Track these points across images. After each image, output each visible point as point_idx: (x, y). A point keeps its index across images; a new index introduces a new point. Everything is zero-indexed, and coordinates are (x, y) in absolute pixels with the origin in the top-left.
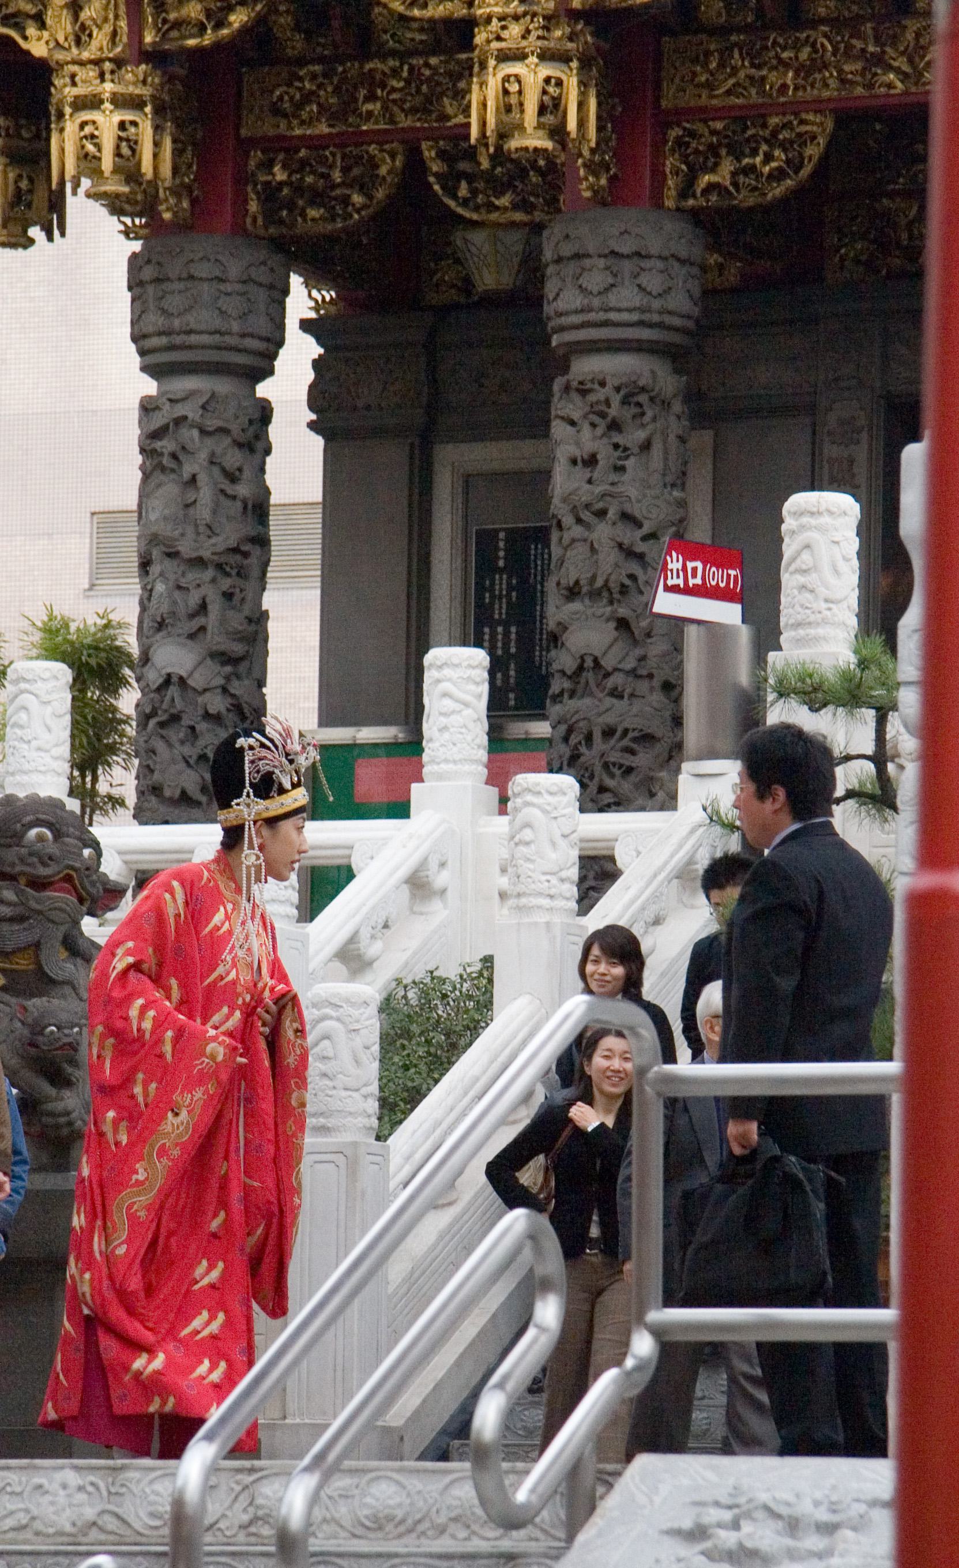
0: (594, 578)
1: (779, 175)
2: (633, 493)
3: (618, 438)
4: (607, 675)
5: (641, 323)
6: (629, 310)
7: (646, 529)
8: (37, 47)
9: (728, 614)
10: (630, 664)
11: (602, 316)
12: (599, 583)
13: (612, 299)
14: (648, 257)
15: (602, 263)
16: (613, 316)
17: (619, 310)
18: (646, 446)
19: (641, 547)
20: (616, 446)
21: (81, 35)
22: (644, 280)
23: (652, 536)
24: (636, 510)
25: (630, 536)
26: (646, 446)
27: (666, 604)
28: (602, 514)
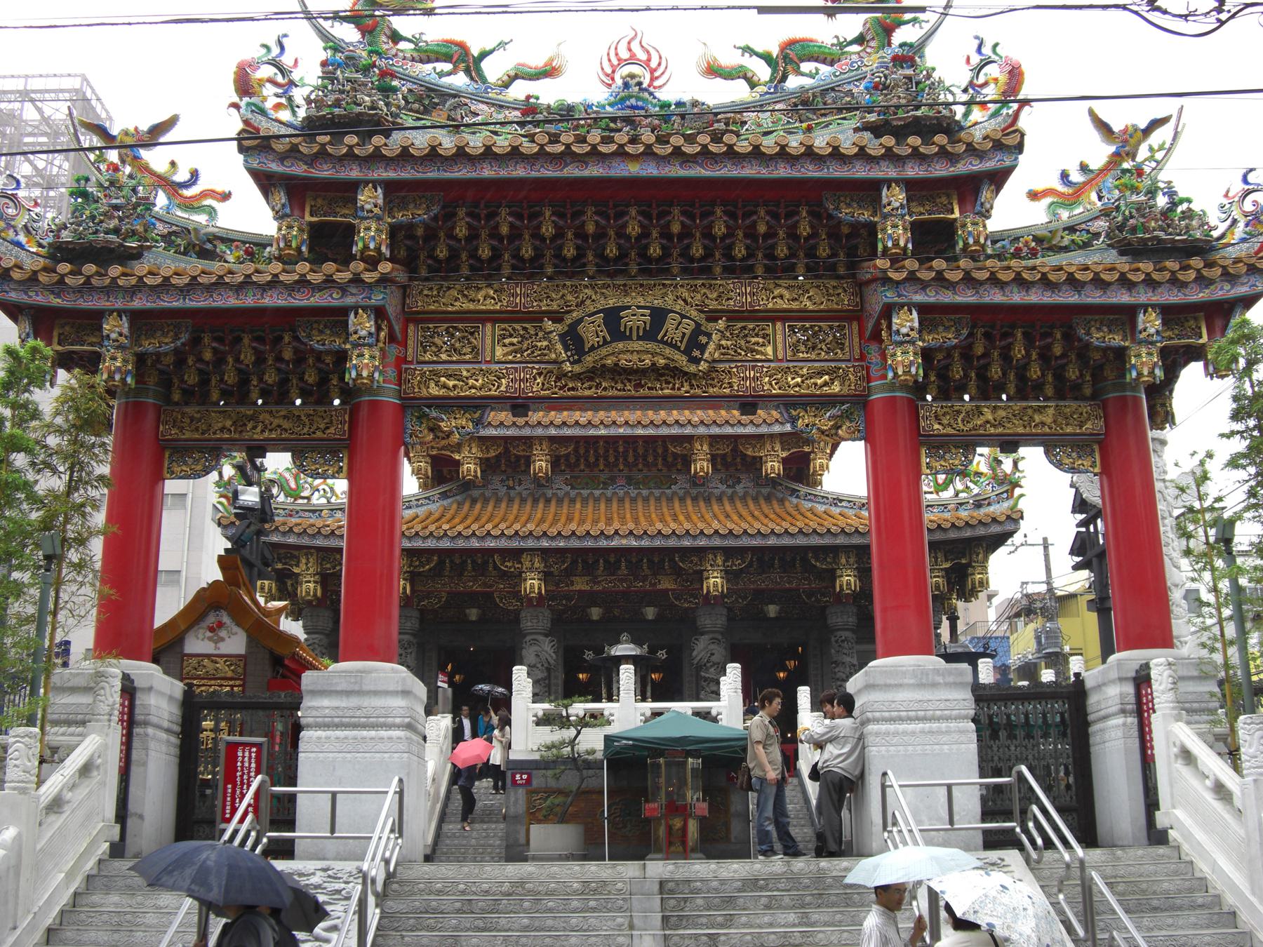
8: (296, 570)
9: (446, 686)
21: (308, 569)
27: (440, 684)
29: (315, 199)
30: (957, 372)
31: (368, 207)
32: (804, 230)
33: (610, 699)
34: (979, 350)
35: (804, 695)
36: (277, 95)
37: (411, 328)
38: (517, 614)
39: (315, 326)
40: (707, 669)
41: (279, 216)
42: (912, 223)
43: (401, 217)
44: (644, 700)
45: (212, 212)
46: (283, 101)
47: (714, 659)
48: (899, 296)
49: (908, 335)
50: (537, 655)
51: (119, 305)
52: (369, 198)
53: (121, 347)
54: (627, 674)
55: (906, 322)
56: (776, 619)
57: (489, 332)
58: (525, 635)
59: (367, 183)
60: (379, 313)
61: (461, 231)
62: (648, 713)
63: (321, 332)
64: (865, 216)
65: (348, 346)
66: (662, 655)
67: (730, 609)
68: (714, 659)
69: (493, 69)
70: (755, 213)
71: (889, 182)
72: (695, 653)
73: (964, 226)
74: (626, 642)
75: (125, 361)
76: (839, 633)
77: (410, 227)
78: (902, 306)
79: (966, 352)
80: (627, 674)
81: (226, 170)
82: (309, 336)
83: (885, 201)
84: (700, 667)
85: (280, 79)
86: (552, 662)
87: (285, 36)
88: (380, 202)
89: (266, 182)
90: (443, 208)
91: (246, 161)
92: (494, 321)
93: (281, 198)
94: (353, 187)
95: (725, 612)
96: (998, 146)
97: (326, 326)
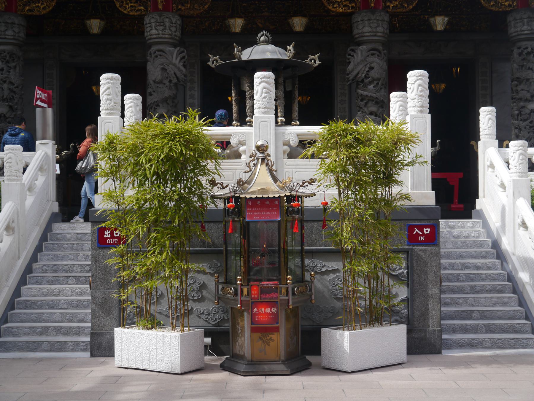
0: (3, 96)
1: (44, 8)
2: (12, 77)
3: (9, 65)
4: (7, 118)
5: (14, 39)
6: (11, 36)
7: (16, 85)
10: (12, 116)
11: (4, 36)
12: (5, 97)
13: (7, 33)
14: (15, 24)
15: (4, 24)
16: (7, 37)
17: (8, 35)
18: (15, 67)
19: (15, 90)
20: (8, 66)
22: (14, 29)
23: (17, 87)
24: (13, 81)
25: (12, 87)
26: (15, 67)
28: (5, 82)
33: (243, 121)
35: (487, 117)
38: (140, 19)
40: (365, 86)
44: (288, 122)
47: (374, 74)
50: (164, 69)
54: (263, 84)
56: (446, 30)
58: (150, 47)
62: (294, 142)
66: (314, 60)
67: (393, 16)
68: (373, 74)
72: (350, 67)
74: (266, 42)
76: (524, 44)
80: (263, 84)
84: (359, 82)
86: (181, 76)
95: (387, 18)
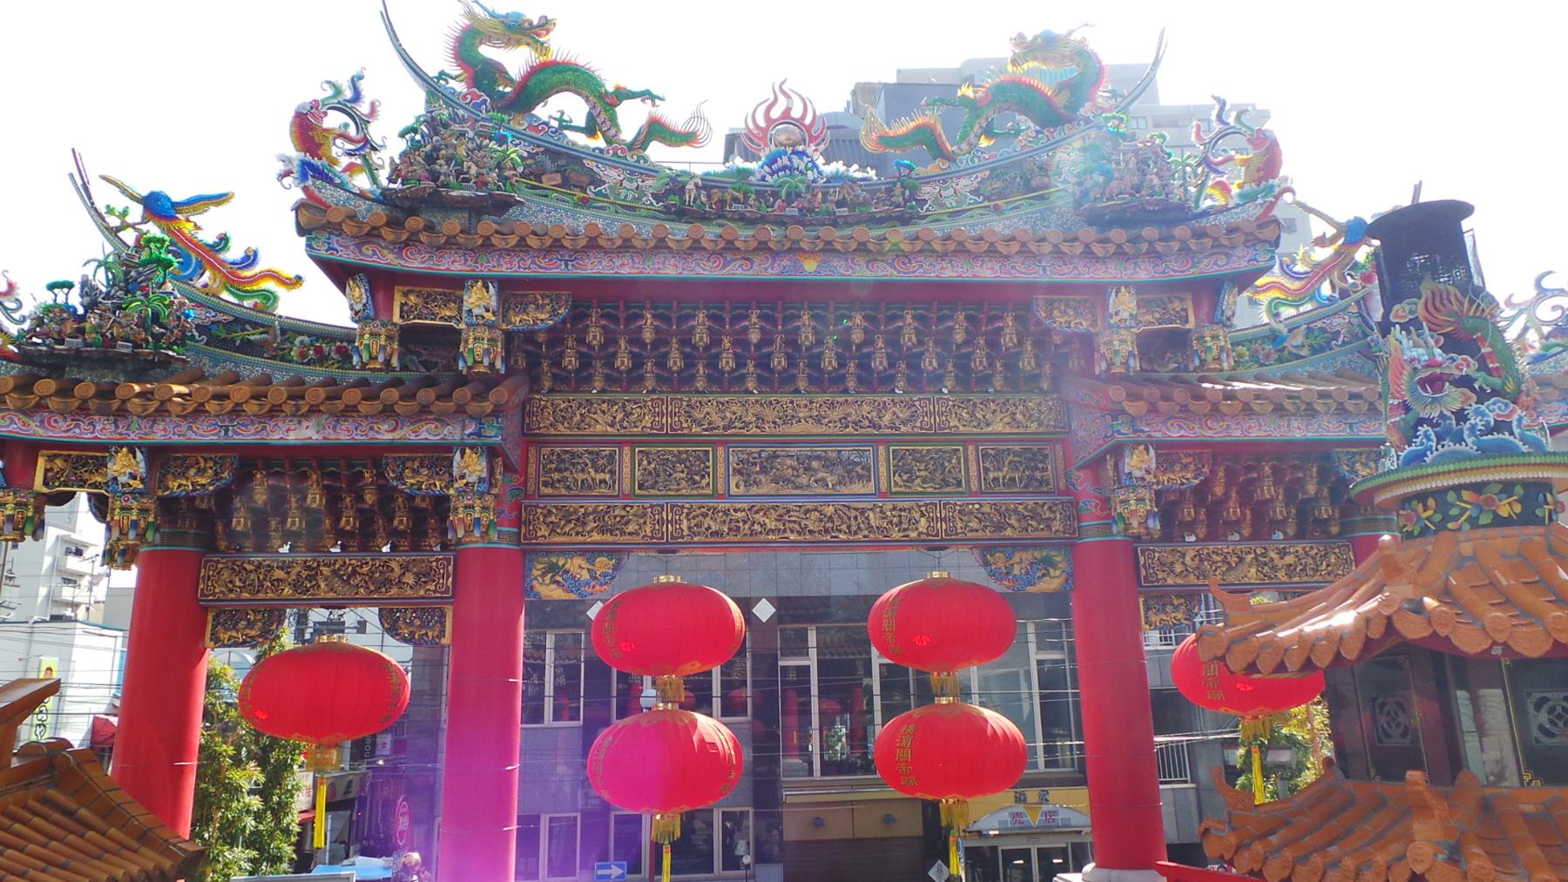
29: (406, 294)
30: (1188, 513)
31: (476, 311)
32: (1008, 339)
34: (1219, 490)
36: (350, 154)
37: (532, 450)
39: (408, 464)
41: (357, 315)
42: (1138, 336)
43: (518, 320)
45: (270, 298)
46: (359, 161)
48: (1135, 431)
49: (1143, 479)
51: (133, 438)
52: (479, 300)
53: (135, 494)
55: (1137, 463)
57: (627, 459)
59: (476, 279)
60: (492, 452)
61: (595, 336)
63: (416, 472)
64: (1084, 325)
65: (452, 491)
69: (630, 119)
70: (951, 317)
71: (1118, 287)
73: (1201, 338)
75: (143, 511)
77: (529, 336)
78: (1139, 444)
79: (1200, 492)
81: (284, 250)
82: (400, 478)
83: (1111, 309)
85: (352, 131)
87: (361, 78)
88: (493, 303)
89: (340, 274)
90: (574, 307)
91: (309, 246)
92: (632, 444)
93: (359, 291)
94: (457, 284)
96: (1252, 240)
97: (422, 465)
